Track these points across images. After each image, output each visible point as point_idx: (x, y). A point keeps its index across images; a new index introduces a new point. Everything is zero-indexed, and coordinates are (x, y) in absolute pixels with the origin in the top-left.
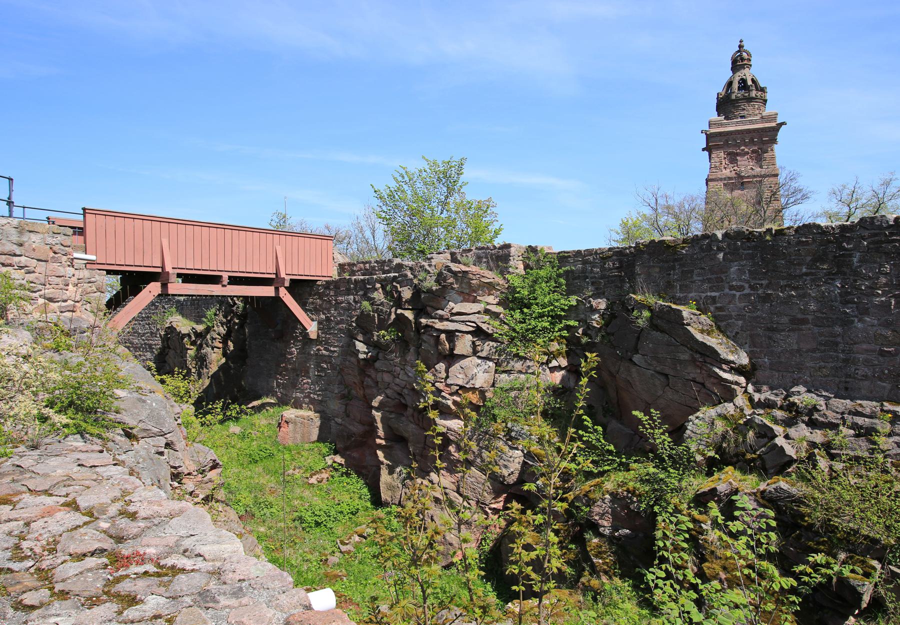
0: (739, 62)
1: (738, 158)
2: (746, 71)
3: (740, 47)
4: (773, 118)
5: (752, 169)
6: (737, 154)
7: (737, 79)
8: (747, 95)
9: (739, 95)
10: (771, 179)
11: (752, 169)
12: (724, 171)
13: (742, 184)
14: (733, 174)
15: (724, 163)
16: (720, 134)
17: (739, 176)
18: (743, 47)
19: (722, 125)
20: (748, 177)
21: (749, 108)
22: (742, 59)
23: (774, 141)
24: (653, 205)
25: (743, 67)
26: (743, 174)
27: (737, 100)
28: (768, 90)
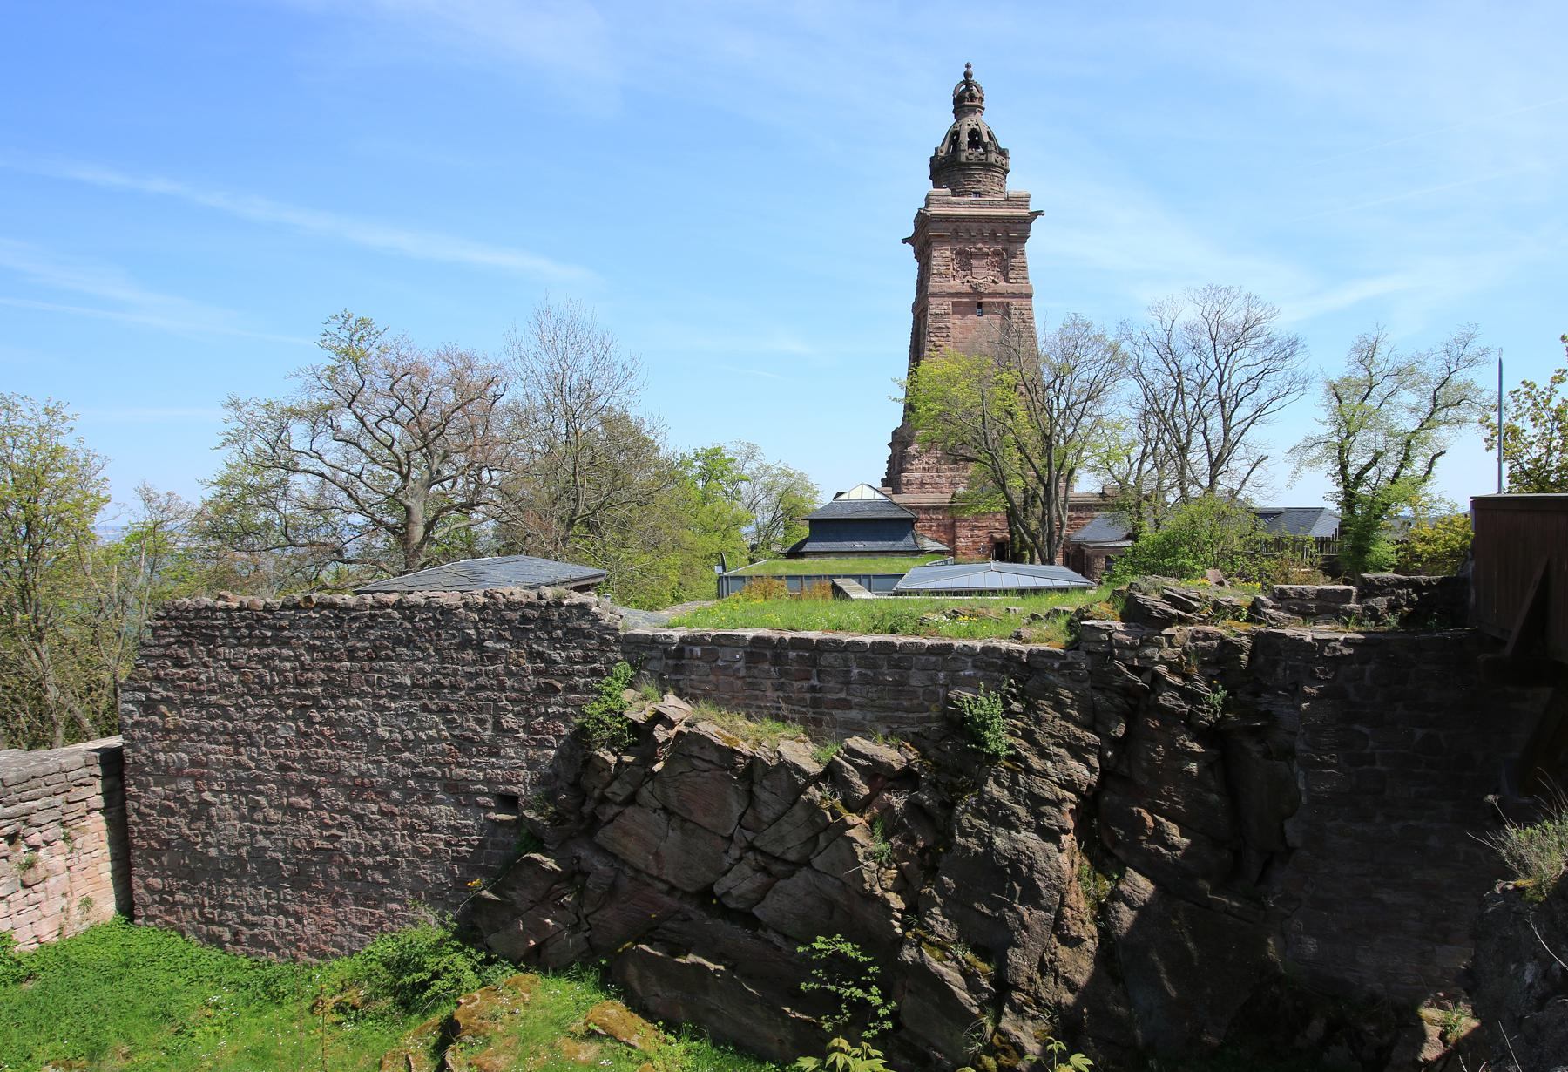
1: (973, 261)
5: (994, 282)
6: (971, 255)
8: (983, 157)
11: (994, 282)
12: (952, 282)
13: (980, 305)
14: (966, 288)
15: (951, 267)
16: (947, 219)
17: (975, 291)
19: (947, 203)
20: (989, 295)
23: (1023, 238)
26: (982, 289)
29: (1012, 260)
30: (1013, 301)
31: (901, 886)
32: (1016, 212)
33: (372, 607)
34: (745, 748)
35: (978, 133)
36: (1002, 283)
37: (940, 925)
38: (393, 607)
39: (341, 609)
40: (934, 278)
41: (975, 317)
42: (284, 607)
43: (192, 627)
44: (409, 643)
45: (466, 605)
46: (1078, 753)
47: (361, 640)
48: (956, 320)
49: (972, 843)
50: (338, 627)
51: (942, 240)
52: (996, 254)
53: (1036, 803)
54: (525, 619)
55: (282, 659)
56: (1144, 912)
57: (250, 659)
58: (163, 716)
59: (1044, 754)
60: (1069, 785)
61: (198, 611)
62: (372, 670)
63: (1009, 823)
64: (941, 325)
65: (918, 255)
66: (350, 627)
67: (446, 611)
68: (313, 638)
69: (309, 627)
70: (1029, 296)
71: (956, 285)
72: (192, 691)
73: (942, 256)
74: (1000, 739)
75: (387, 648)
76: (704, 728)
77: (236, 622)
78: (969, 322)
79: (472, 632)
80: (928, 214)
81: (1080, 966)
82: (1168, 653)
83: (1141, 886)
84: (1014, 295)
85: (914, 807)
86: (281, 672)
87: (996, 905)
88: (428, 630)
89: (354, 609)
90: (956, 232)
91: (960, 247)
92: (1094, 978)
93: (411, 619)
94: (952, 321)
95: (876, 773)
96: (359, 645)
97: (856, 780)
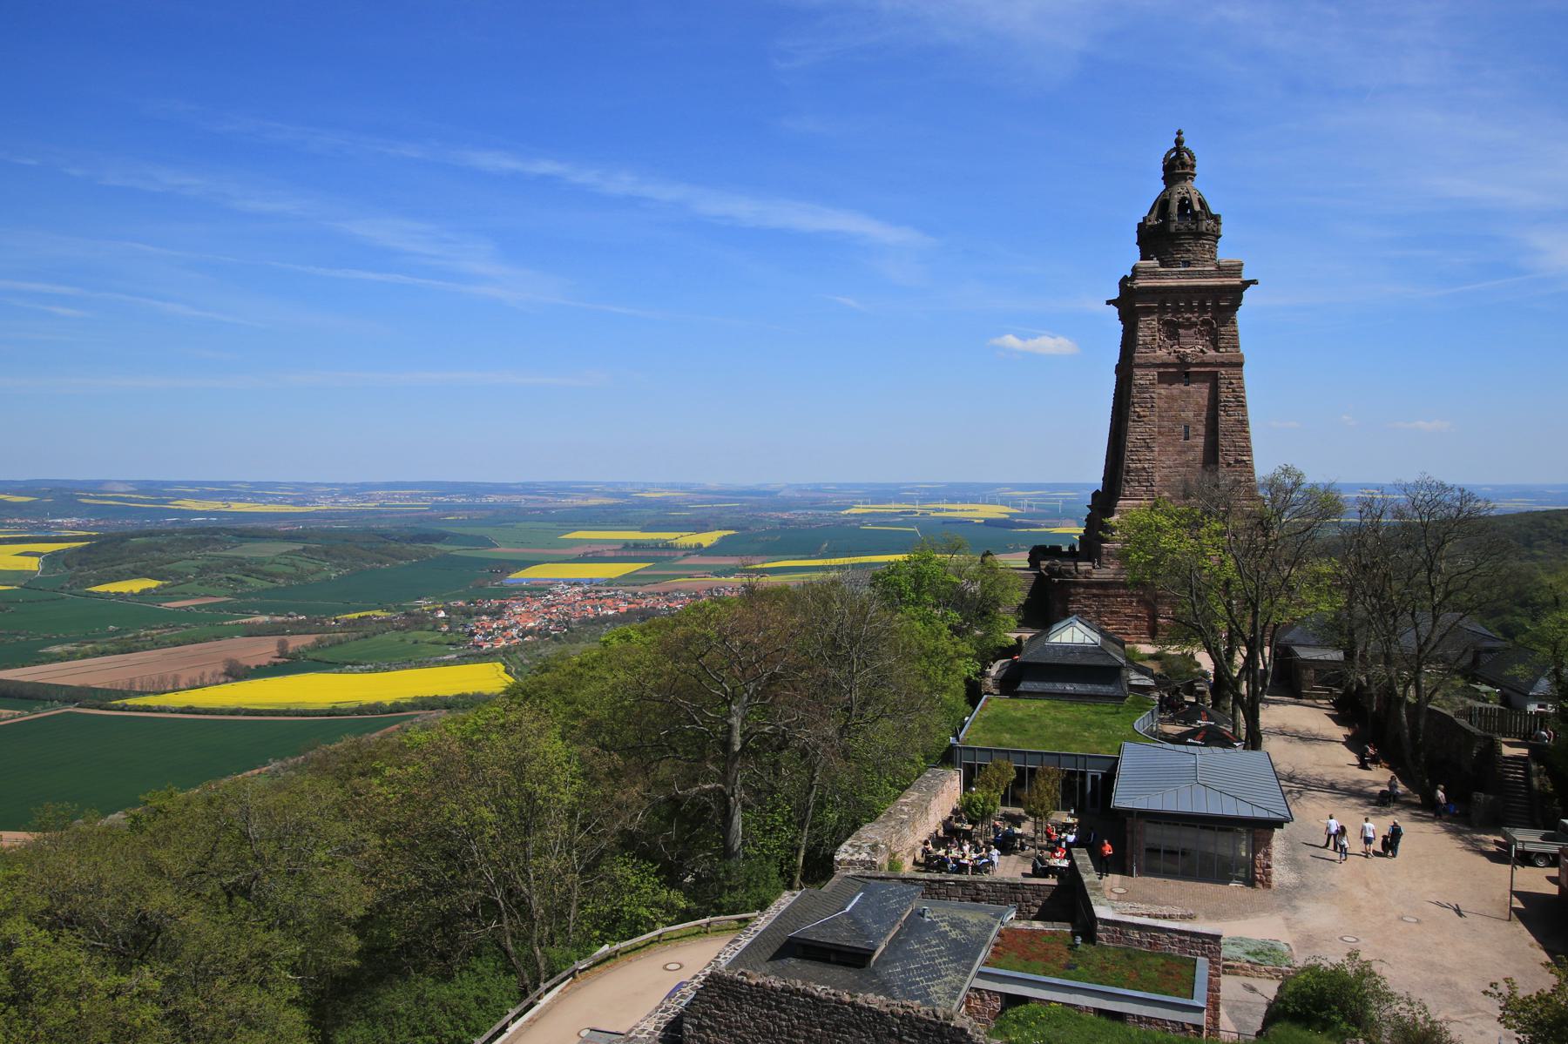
0: (1177, 167)
1: (1181, 331)
2: (1189, 184)
3: (1179, 142)
4: (1235, 270)
5: (1202, 351)
7: (1176, 198)
9: (1182, 227)
10: (1230, 370)
11: (1202, 351)
12: (1159, 353)
13: (1187, 374)
14: (1173, 358)
15: (1157, 338)
17: (1182, 361)
18: (1182, 142)
19: (1155, 275)
22: (1184, 165)
24: (1423, 640)
27: (1178, 234)
28: (1222, 220)
29: (1222, 329)
33: (836, 1002)
35: (1190, 205)
36: (1211, 353)
38: (848, 1005)
39: (817, 1000)
41: (1182, 386)
42: (783, 990)
43: (727, 989)
44: (858, 1028)
45: (892, 1012)
47: (828, 1019)
48: (1163, 390)
50: (815, 1009)
51: (1148, 311)
52: (1205, 322)
54: (927, 1029)
55: (781, 1019)
57: (761, 1015)
58: (708, 1036)
61: (731, 982)
62: (835, 1037)
64: (1147, 395)
65: (1122, 318)
66: (822, 1011)
67: (881, 1015)
68: (799, 1011)
69: (797, 1005)
71: (1162, 354)
72: (726, 1025)
73: (1148, 327)
75: (844, 1027)
77: (755, 994)
78: (1175, 392)
79: (895, 1029)
80: (1135, 287)
86: (779, 1027)
88: (869, 1022)
89: (825, 1001)
90: (1163, 304)
91: (1168, 317)
93: (859, 1014)
94: (1158, 391)
96: (827, 1021)
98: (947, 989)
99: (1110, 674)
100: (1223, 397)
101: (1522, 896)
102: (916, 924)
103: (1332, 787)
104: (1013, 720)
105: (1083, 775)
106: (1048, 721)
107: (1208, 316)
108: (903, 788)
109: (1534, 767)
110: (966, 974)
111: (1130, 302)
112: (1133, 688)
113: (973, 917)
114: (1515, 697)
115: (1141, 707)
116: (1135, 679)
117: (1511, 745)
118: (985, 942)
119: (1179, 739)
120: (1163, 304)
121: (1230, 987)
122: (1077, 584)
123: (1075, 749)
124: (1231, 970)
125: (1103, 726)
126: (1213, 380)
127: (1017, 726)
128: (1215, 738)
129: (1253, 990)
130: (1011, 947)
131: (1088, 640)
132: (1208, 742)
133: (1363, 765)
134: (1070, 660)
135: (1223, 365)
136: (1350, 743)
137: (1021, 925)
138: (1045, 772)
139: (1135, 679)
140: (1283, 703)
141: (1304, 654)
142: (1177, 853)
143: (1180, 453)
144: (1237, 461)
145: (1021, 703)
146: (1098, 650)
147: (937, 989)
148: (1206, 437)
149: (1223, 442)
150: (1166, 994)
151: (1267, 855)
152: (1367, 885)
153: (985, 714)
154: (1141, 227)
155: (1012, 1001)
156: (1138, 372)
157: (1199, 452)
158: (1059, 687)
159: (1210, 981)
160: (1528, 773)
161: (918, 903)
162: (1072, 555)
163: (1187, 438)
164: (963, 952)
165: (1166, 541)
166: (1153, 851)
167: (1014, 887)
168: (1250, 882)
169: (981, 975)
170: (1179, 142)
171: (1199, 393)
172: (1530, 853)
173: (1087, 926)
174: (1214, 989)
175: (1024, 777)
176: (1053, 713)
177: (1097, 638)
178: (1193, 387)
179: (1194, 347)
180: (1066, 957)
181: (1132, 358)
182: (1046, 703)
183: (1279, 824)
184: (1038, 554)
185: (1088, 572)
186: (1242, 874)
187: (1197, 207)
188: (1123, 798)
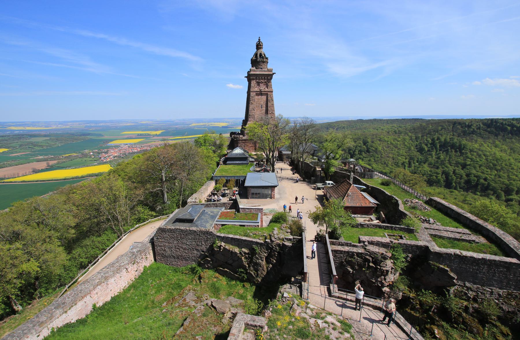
0: (259, 46)
1: (260, 84)
2: (261, 50)
3: (259, 40)
4: (271, 70)
6: (260, 83)
10: (271, 93)
12: (256, 89)
13: (262, 94)
14: (258, 90)
17: (261, 91)
19: (255, 71)
20: (264, 92)
21: (263, 66)
22: (260, 45)
25: (261, 48)
27: (259, 62)
30: (269, 93)
31: (248, 264)
32: (270, 73)
34: (231, 250)
35: (262, 55)
37: (252, 268)
40: (252, 88)
46: (265, 253)
48: (257, 97)
49: (255, 261)
51: (253, 79)
52: (265, 82)
53: (261, 258)
56: (271, 269)
59: (262, 253)
60: (264, 256)
63: (258, 259)
65: (248, 81)
70: (272, 92)
71: (256, 89)
73: (253, 83)
74: (258, 251)
76: (227, 247)
78: (259, 98)
81: (265, 273)
82: (275, 244)
83: (271, 266)
84: (269, 92)
85: (249, 257)
87: (257, 267)
90: (256, 78)
91: (258, 81)
92: (266, 274)
95: (245, 253)
97: (243, 254)
98: (210, 225)
99: (245, 159)
100: (269, 99)
101: (317, 195)
102: (203, 213)
103: (288, 178)
104: (225, 170)
105: (240, 180)
106: (233, 170)
107: (266, 81)
108: (202, 186)
109: (322, 172)
110: (214, 221)
111: (250, 77)
112: (250, 161)
113: (215, 210)
114: (320, 159)
115: (251, 165)
116: (251, 159)
117: (318, 168)
118: (218, 215)
119: (259, 171)
120: (256, 78)
121: (264, 217)
122: (240, 140)
123: (238, 175)
124: (265, 214)
125: (244, 170)
126: (267, 95)
127: (226, 171)
128: (266, 171)
129: (268, 217)
130: (223, 215)
131: (241, 152)
132: (264, 172)
133: (294, 174)
134: (237, 156)
135: (269, 92)
136: (292, 170)
137: (225, 211)
138: (232, 180)
139: (251, 159)
140: (280, 163)
141: (284, 152)
142: (257, 194)
143: (260, 111)
144: (272, 113)
145: (227, 166)
146: (243, 154)
147: (208, 225)
148: (266, 107)
149: (269, 108)
150: (252, 220)
151: (274, 192)
152: (292, 196)
153: (220, 169)
154: (252, 59)
155: (223, 225)
156: (251, 93)
157: (264, 111)
158: (235, 162)
159: (261, 217)
160: (321, 173)
161: (204, 209)
162: (238, 134)
163: (262, 108)
164: (213, 217)
165: (256, 130)
166: (253, 194)
167: (224, 204)
168: (271, 198)
169: (217, 221)
170: (259, 40)
171: (264, 98)
172: (320, 188)
173: (238, 209)
174: (262, 219)
175: (227, 181)
176: (234, 167)
177: (243, 151)
178: (263, 97)
179: (263, 87)
180: (234, 216)
181: (250, 90)
182: (232, 166)
183: (276, 186)
184: (232, 134)
185: (242, 137)
186: (269, 197)
187: (263, 56)
188: (246, 184)
